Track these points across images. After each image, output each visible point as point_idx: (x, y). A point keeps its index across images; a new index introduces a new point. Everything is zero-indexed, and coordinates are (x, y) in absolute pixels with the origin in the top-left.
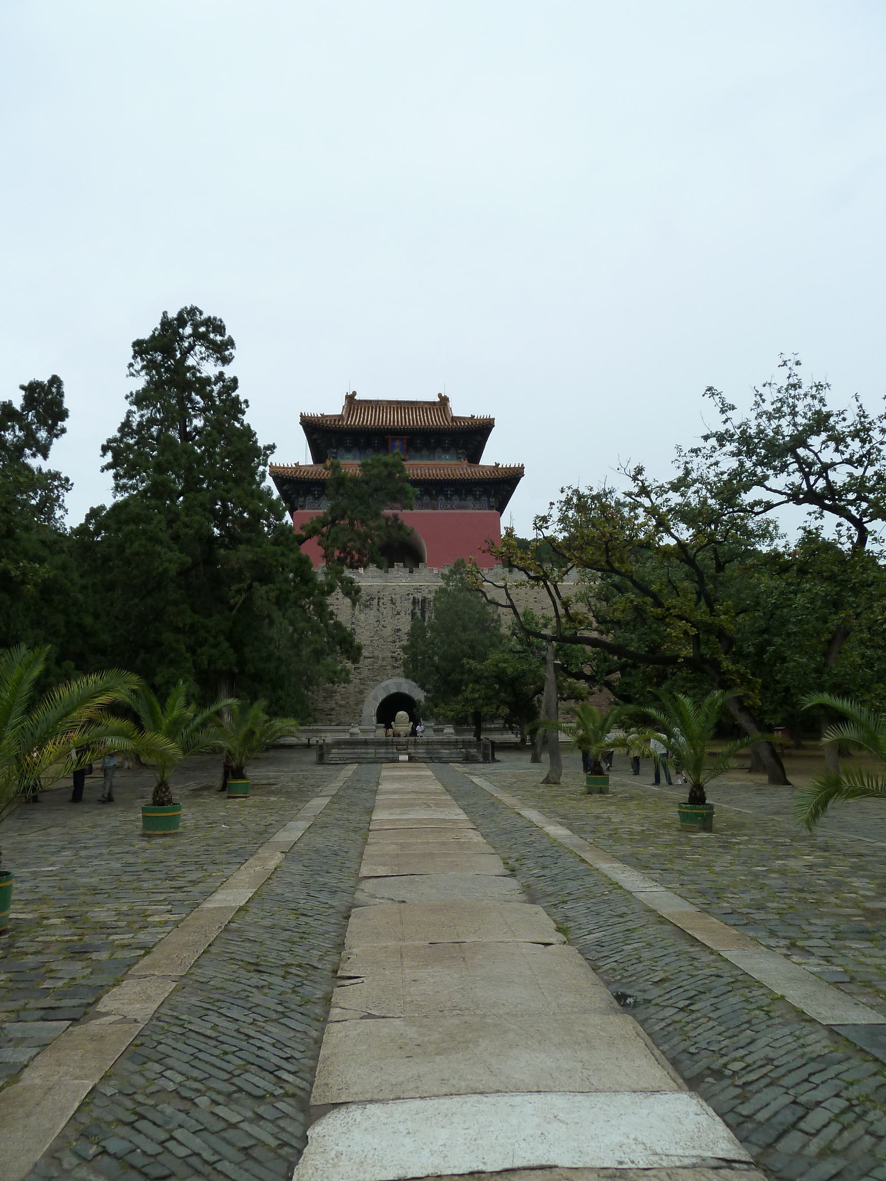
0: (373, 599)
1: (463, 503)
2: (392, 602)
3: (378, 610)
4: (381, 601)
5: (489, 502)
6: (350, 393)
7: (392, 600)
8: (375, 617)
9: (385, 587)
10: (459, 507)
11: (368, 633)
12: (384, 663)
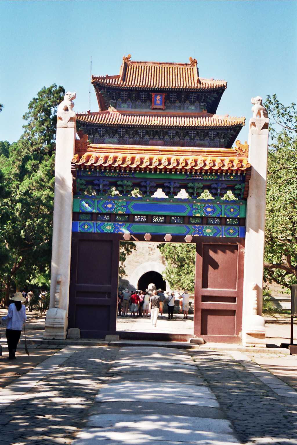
1: (202, 142)
6: (127, 56)
12: (144, 251)
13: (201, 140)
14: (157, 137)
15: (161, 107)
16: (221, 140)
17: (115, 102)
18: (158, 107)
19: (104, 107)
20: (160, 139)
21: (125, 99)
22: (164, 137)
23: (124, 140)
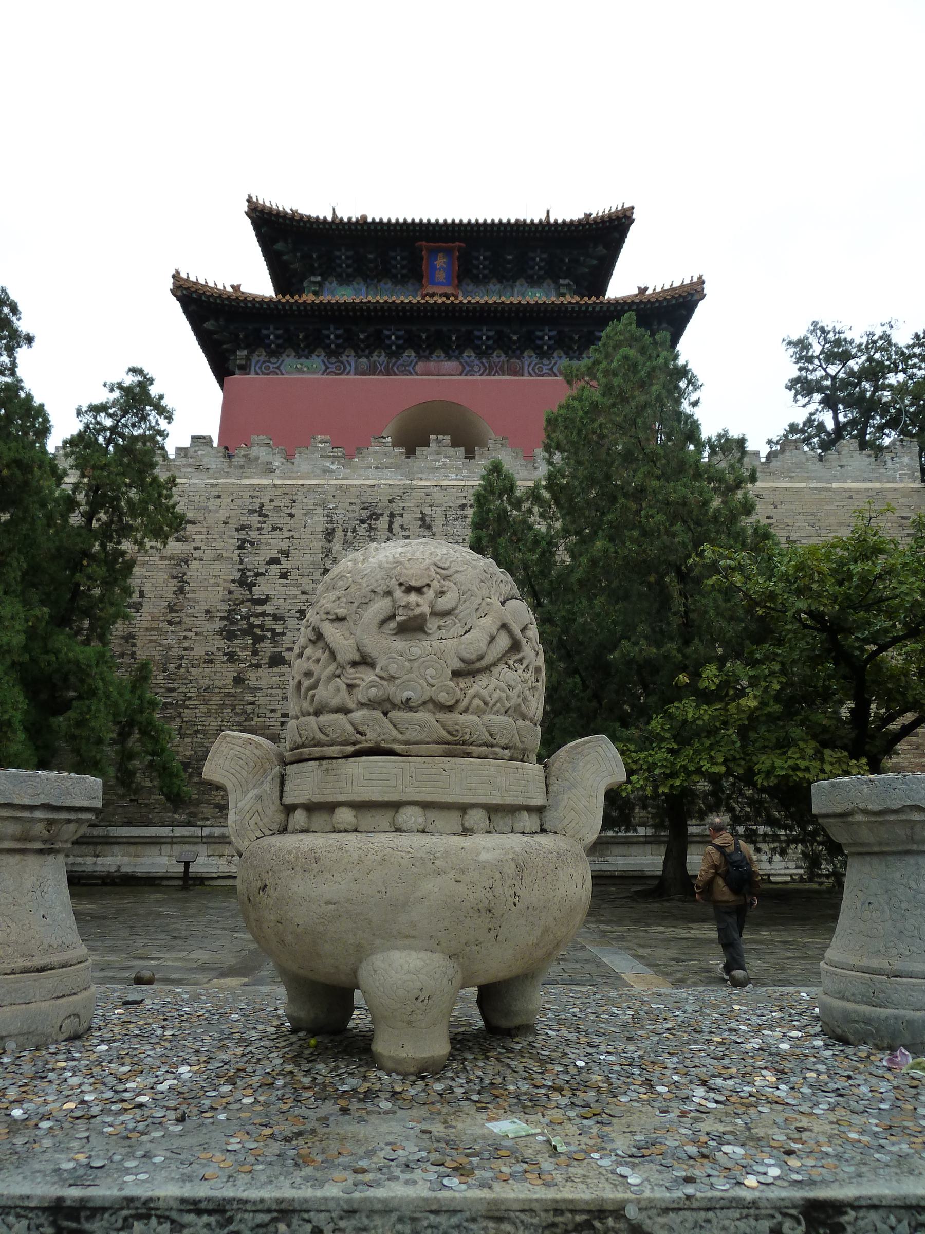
0: (376, 516)
4: (398, 521)
7: (423, 519)
9: (406, 490)
17: (319, 279)
20: (449, 358)
22: (461, 353)
23: (342, 362)
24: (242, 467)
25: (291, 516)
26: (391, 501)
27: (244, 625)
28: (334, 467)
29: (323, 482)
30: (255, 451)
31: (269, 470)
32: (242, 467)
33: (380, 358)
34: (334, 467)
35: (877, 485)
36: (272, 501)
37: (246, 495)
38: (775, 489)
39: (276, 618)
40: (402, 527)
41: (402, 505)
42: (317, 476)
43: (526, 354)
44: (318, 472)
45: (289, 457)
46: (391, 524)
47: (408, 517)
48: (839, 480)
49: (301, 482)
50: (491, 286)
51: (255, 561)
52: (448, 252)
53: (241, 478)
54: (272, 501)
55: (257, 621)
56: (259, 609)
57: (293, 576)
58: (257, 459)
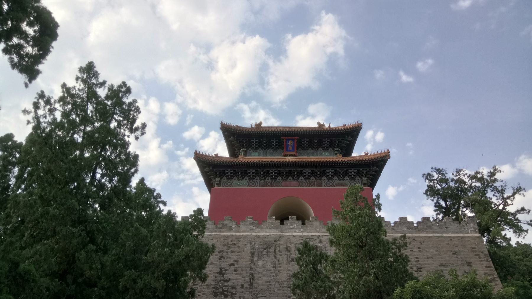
1: (342, 181)
2: (288, 249)
3: (275, 257)
4: (278, 249)
5: (362, 180)
7: (287, 248)
8: (272, 263)
9: (280, 237)
10: (338, 185)
11: (265, 278)
13: (340, 180)
14: (290, 178)
15: (293, 153)
16: (363, 178)
17: (245, 149)
18: (290, 153)
19: (233, 152)
21: (256, 148)
22: (299, 178)
24: (221, 228)
25: (239, 247)
26: (275, 241)
27: (220, 290)
28: (254, 228)
29: (250, 234)
30: (226, 222)
31: (231, 229)
32: (221, 228)
33: (268, 180)
34: (254, 228)
35: (462, 235)
36: (231, 241)
37: (222, 239)
38: (421, 237)
39: (233, 288)
40: (279, 251)
41: (279, 242)
42: (248, 232)
43: (323, 178)
44: (248, 230)
45: (238, 224)
46: (275, 250)
47: (281, 247)
48: (446, 233)
49: (242, 234)
50: (309, 151)
51: (224, 265)
52: (293, 140)
53: (220, 232)
54: (231, 241)
55: (225, 289)
56: (226, 284)
57: (240, 270)
58: (226, 225)
